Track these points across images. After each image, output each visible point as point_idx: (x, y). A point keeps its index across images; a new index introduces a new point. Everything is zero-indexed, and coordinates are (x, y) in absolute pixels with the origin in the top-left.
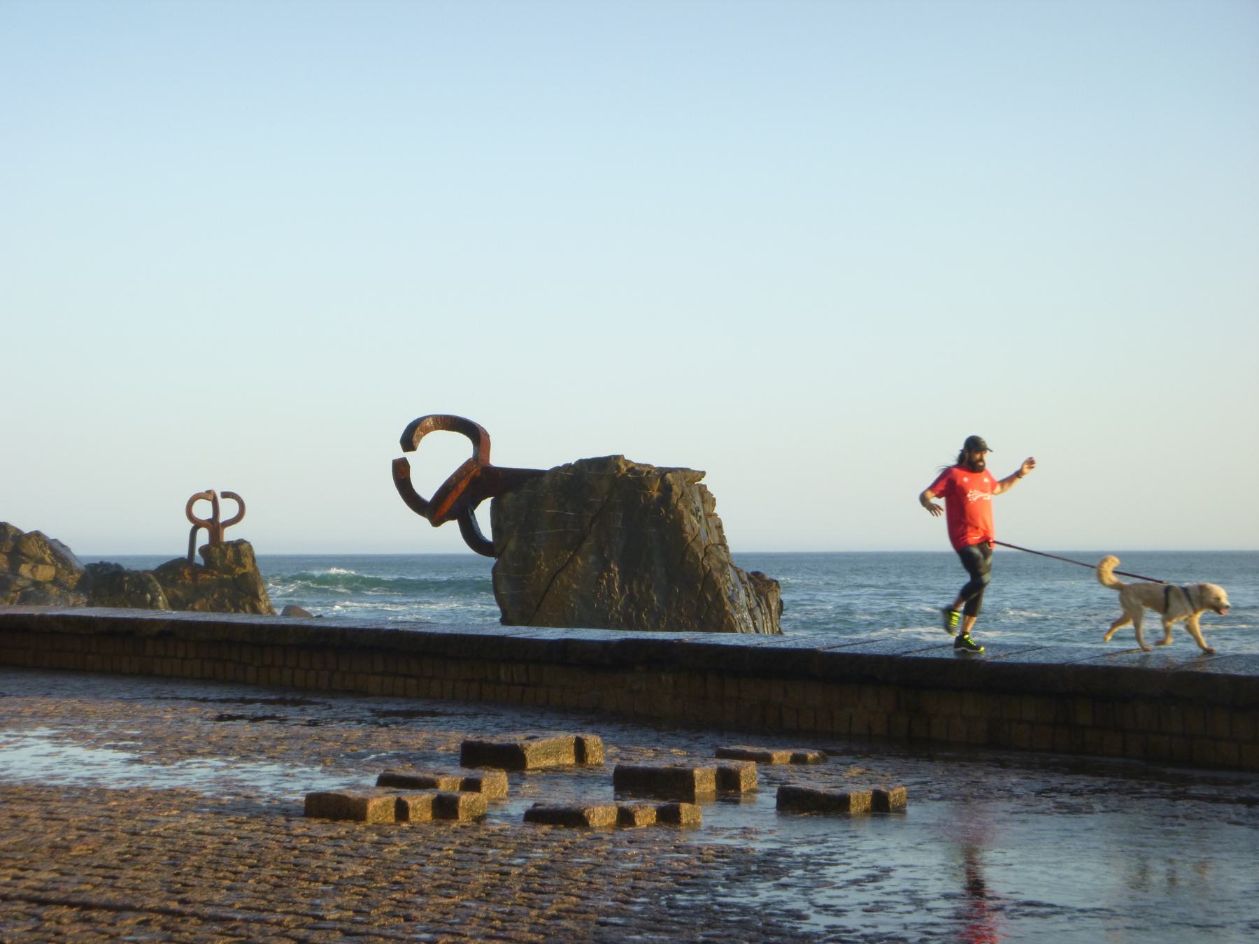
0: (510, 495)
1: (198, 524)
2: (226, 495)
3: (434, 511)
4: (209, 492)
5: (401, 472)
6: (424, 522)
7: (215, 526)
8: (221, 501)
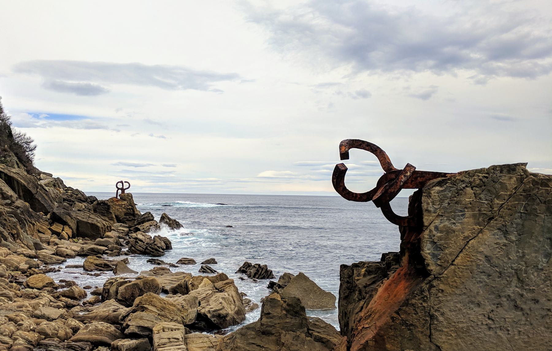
2: (126, 182)
7: (123, 190)
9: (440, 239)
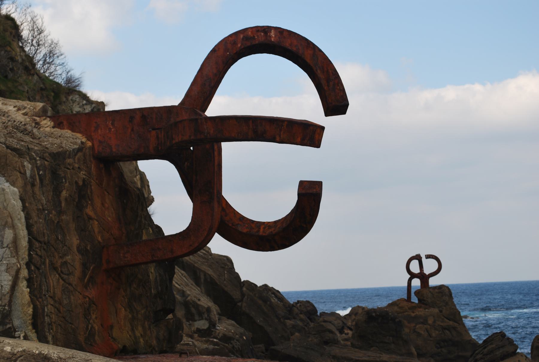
1: (413, 276)
2: (428, 257)
4: (417, 255)
7: (424, 278)
8: (424, 260)
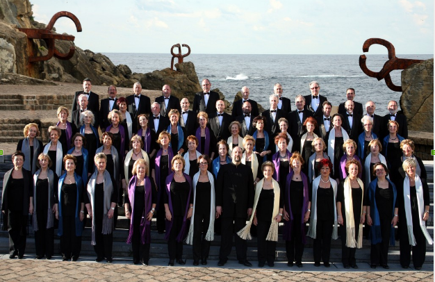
0: (409, 70)
1: (174, 56)
3: (378, 76)
5: (362, 61)
6: (376, 79)
7: (180, 57)
9: (410, 98)
